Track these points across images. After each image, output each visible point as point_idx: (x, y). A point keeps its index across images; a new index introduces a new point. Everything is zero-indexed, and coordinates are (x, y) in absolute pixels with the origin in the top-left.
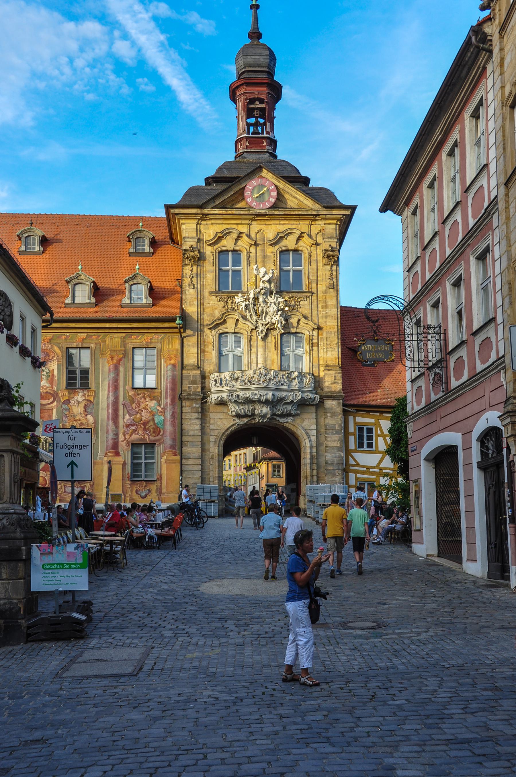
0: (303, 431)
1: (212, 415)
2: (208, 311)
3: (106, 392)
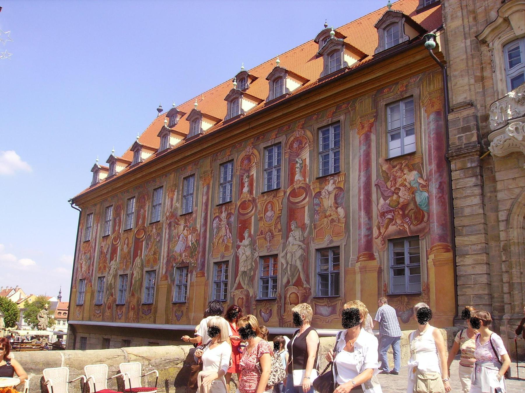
1: (499, 176)
2: (481, 18)
3: (357, 173)
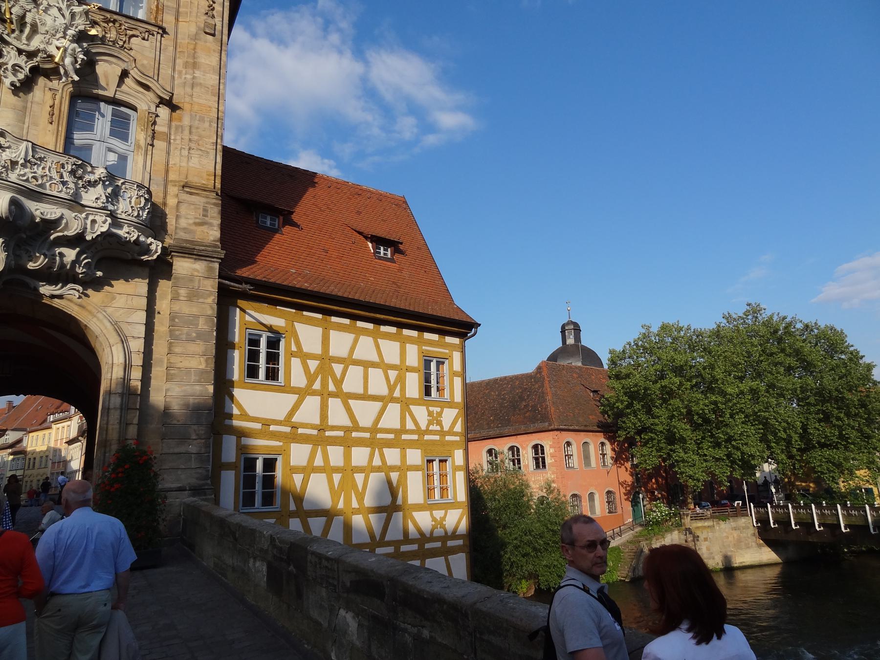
0: (108, 325)
